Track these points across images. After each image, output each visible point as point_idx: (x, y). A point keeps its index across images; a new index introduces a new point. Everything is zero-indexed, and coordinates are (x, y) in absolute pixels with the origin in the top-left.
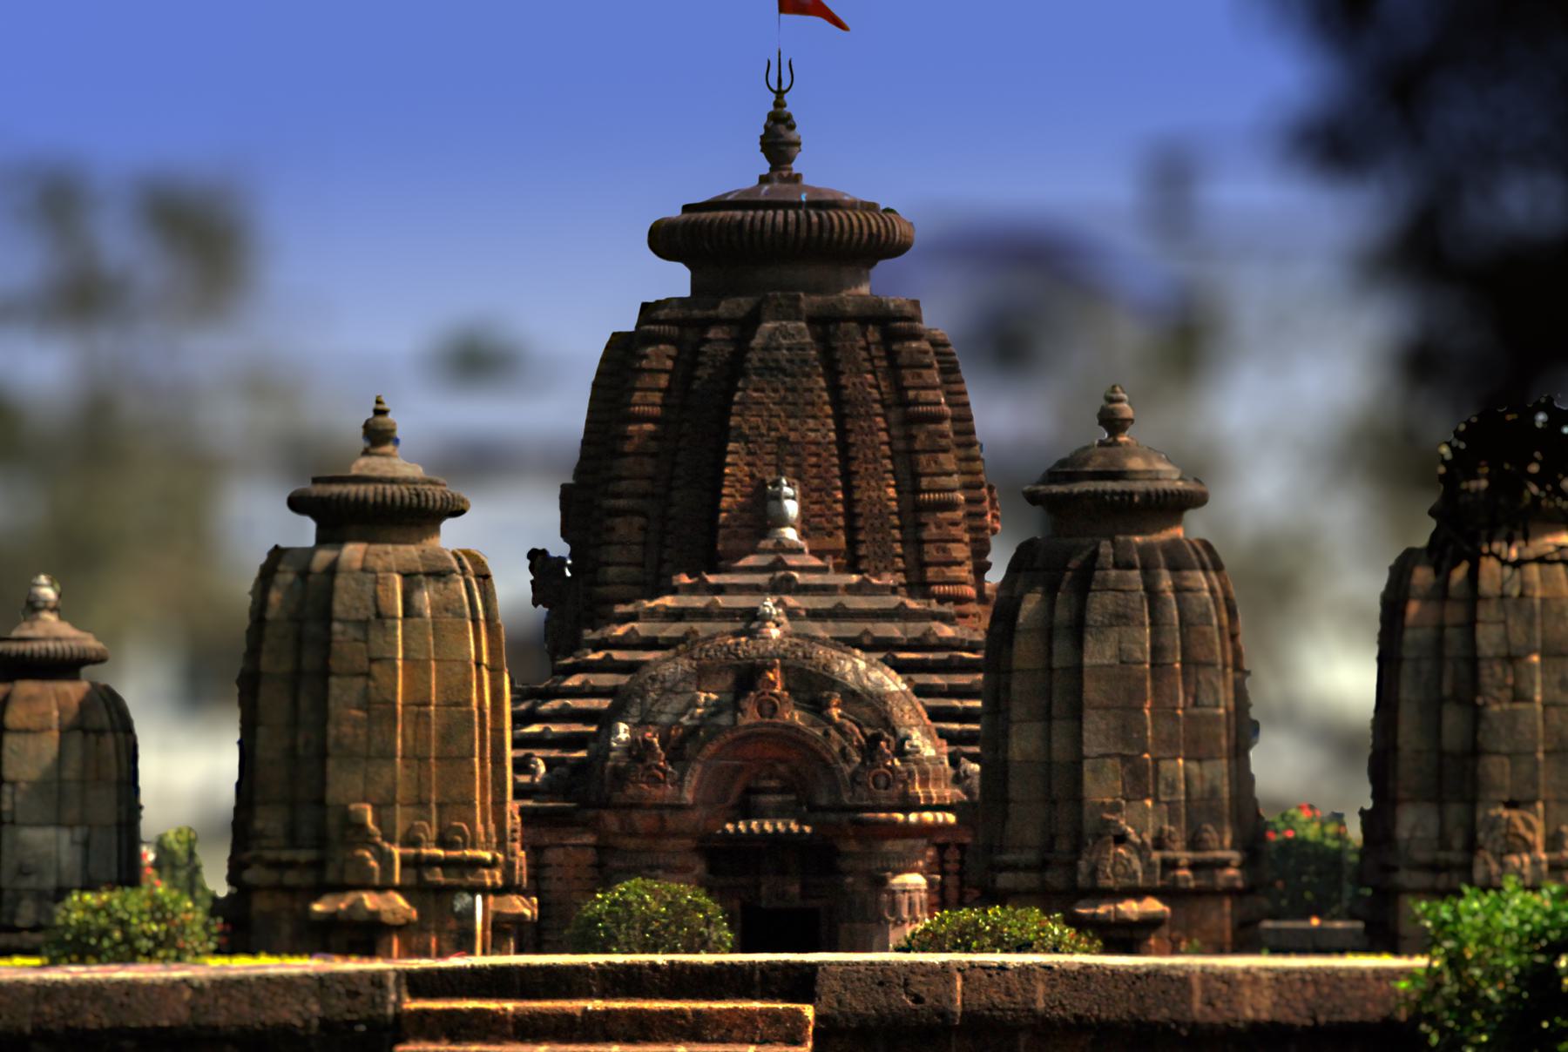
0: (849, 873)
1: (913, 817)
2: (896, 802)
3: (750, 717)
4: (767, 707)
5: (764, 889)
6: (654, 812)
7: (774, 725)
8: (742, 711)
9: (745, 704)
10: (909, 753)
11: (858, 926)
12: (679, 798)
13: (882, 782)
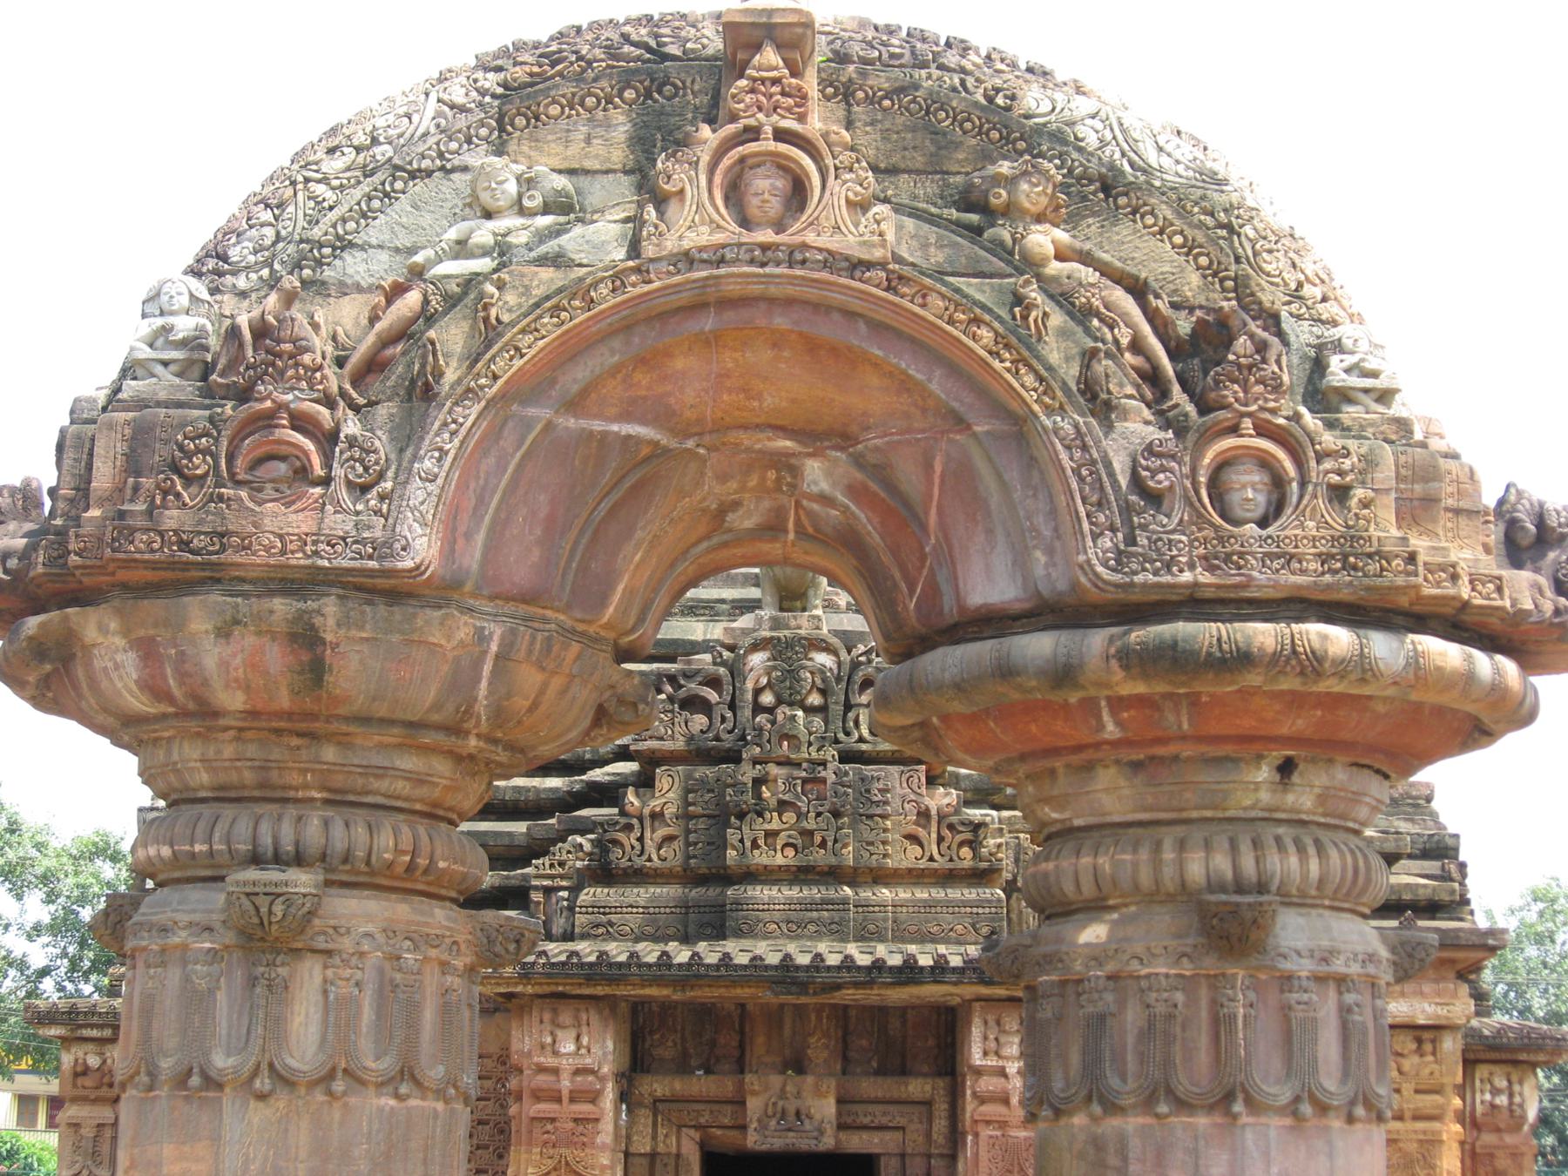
0: (1095, 907)
1: (1384, 647)
2: (1305, 577)
3: (696, 222)
4: (766, 188)
5: (754, 1105)
6: (281, 607)
7: (795, 255)
8: (662, 202)
9: (673, 172)
10: (1347, 396)
11: (1132, 1123)
12: (383, 549)
13: (1249, 490)
